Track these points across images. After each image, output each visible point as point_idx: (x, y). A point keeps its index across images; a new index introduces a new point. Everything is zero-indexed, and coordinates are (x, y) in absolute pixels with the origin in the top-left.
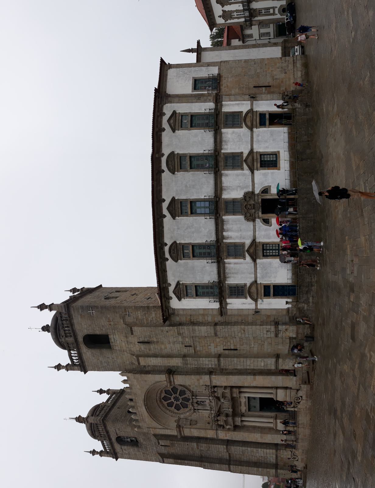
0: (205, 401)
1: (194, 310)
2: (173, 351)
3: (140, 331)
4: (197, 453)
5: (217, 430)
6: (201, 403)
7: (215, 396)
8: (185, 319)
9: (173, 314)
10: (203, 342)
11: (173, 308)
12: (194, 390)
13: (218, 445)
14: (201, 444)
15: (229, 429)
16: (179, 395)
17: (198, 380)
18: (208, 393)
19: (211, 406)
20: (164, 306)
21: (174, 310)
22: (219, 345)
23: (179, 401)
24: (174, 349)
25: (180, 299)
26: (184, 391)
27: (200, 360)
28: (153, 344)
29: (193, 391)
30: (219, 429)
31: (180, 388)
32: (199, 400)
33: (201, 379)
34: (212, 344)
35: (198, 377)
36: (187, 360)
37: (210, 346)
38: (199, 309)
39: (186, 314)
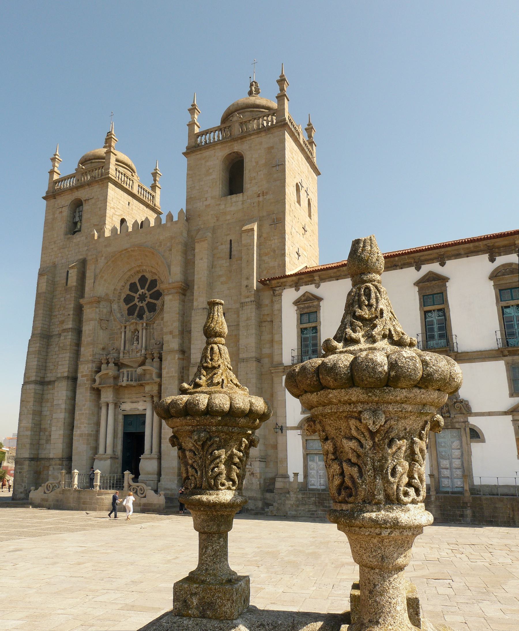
0: (138, 343)
1: (280, 327)
2: (218, 294)
4: (55, 330)
5: (93, 362)
6: (136, 337)
7: (146, 358)
8: (266, 314)
9: (274, 293)
12: (156, 326)
13: (69, 364)
14: (70, 337)
15: (94, 381)
16: (148, 302)
17: (171, 333)
18: (151, 348)
19: (130, 353)
20: (285, 280)
21: (280, 295)
23: (139, 302)
25: (297, 303)
28: (228, 264)
30: (94, 365)
31: (158, 302)
33: (173, 337)
35: (176, 332)
38: (282, 334)
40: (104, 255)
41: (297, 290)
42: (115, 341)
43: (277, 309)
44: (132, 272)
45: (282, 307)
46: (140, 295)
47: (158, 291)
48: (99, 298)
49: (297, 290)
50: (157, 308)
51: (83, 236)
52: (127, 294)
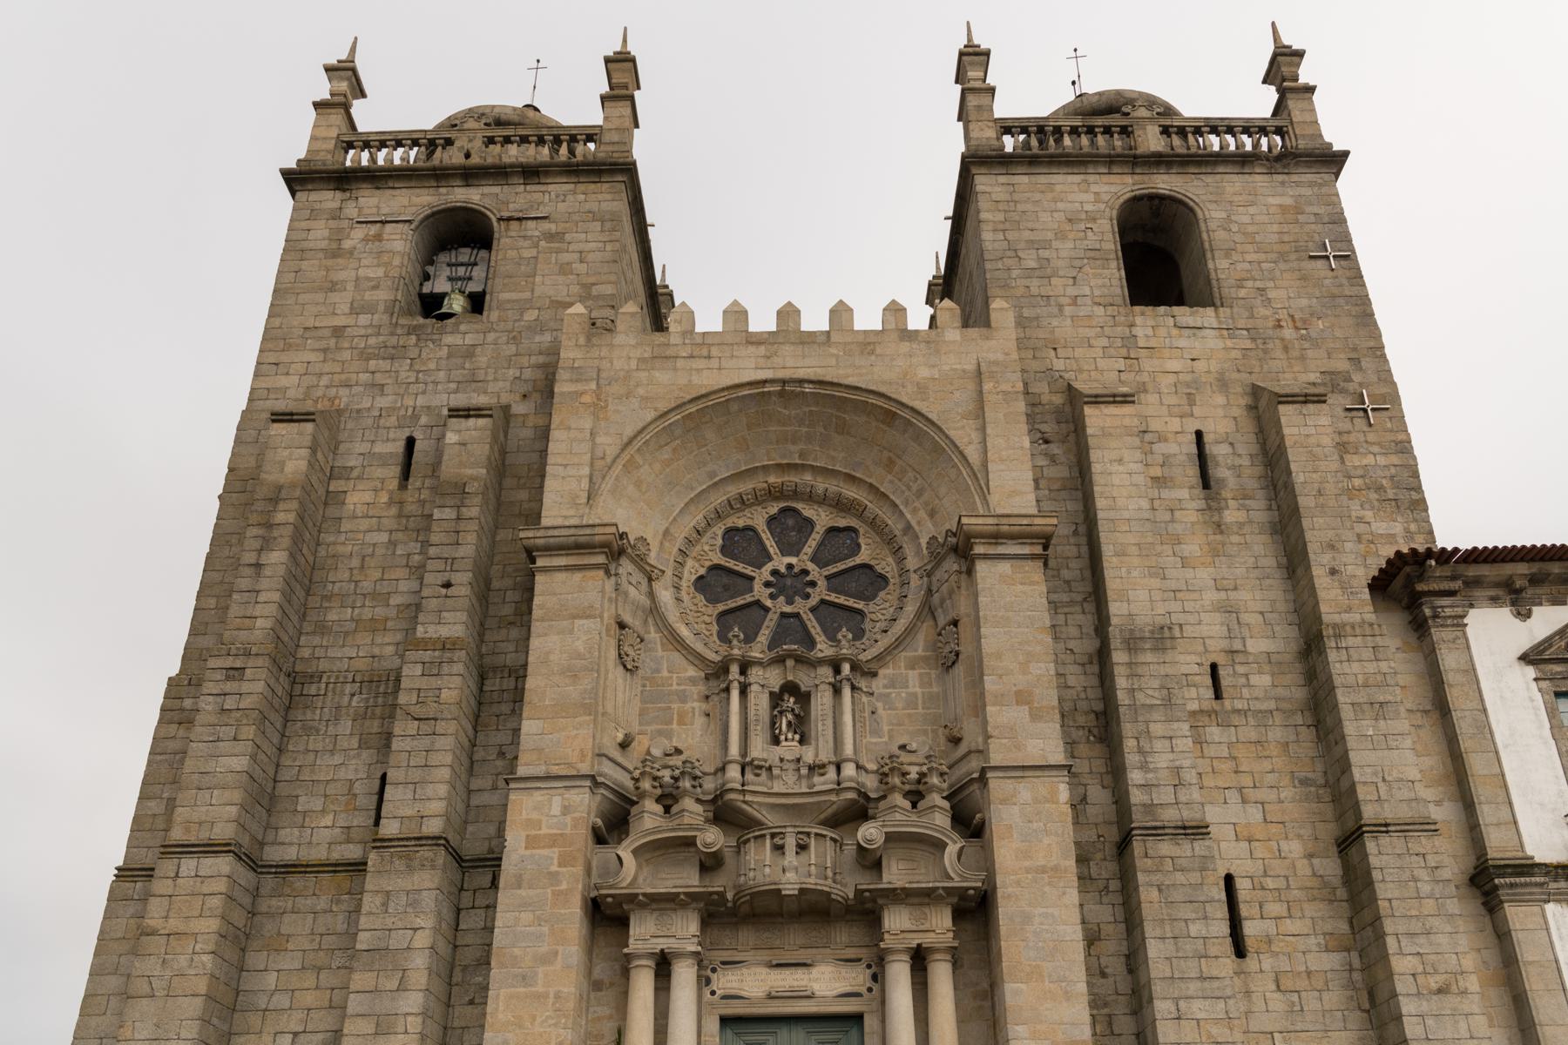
1: (1484, 728)
3: (1312, 440)
5: (595, 782)
9: (1435, 616)
10: (1267, 765)
11: (1465, 621)
12: (885, 687)
16: (823, 602)
19: (776, 772)
20: (1484, 570)
22: (1258, 854)
23: (772, 596)
24: (1189, 606)
26: (859, 634)
27: (1175, 725)
29: (875, 675)
32: (822, 701)
34: (1255, 814)
36: (1155, 649)
37: (1244, 801)
38: (1497, 753)
39: (1451, 686)
40: (641, 391)
41: (1524, 615)
42: (675, 726)
43: (1454, 665)
44: (746, 487)
45: (1473, 665)
46: (775, 573)
47: (866, 567)
48: (623, 536)
49: (1524, 615)
50: (867, 625)
51: (492, 330)
52: (708, 564)
